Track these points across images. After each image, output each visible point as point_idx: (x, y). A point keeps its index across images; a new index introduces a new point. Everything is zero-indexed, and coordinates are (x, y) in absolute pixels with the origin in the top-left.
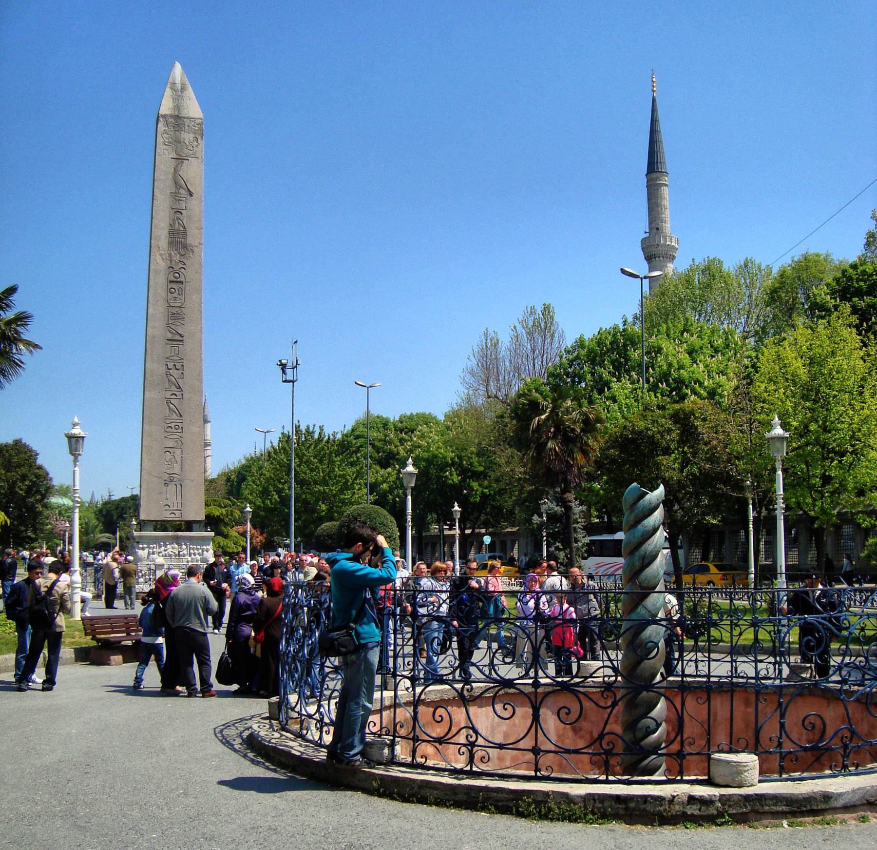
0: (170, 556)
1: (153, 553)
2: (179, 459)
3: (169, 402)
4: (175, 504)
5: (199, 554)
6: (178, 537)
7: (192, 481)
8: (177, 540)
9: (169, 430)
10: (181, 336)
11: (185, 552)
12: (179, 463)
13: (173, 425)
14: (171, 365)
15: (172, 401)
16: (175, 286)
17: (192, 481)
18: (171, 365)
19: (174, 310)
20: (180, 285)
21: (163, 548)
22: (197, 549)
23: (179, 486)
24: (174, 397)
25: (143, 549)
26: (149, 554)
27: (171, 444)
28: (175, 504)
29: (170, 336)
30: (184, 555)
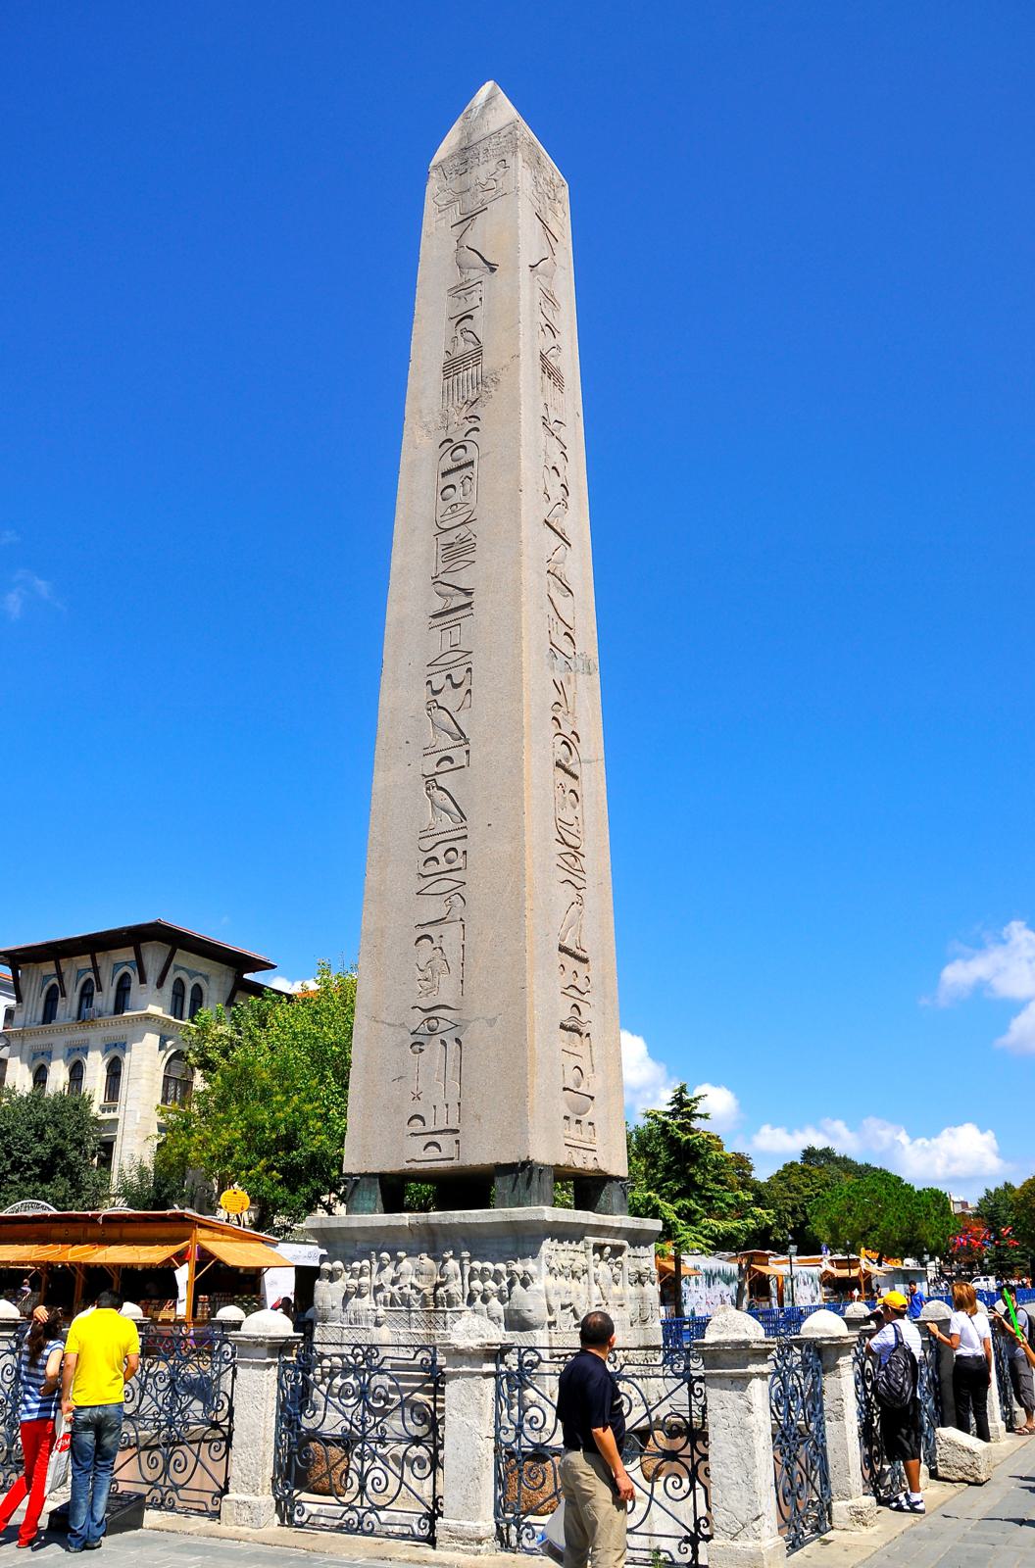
0: (406, 1301)
1: (359, 1294)
2: (453, 955)
3: (430, 781)
4: (442, 1111)
6: (430, 1230)
7: (492, 1022)
8: (433, 1242)
9: (433, 867)
10: (468, 593)
12: (455, 966)
13: (439, 852)
14: (439, 681)
15: (441, 780)
16: (452, 479)
17: (492, 1022)
18: (439, 681)
19: (450, 537)
20: (466, 471)
21: (390, 1272)
23: (452, 1045)
24: (446, 765)
26: (346, 1298)
27: (433, 909)
28: (442, 1111)
29: (439, 604)
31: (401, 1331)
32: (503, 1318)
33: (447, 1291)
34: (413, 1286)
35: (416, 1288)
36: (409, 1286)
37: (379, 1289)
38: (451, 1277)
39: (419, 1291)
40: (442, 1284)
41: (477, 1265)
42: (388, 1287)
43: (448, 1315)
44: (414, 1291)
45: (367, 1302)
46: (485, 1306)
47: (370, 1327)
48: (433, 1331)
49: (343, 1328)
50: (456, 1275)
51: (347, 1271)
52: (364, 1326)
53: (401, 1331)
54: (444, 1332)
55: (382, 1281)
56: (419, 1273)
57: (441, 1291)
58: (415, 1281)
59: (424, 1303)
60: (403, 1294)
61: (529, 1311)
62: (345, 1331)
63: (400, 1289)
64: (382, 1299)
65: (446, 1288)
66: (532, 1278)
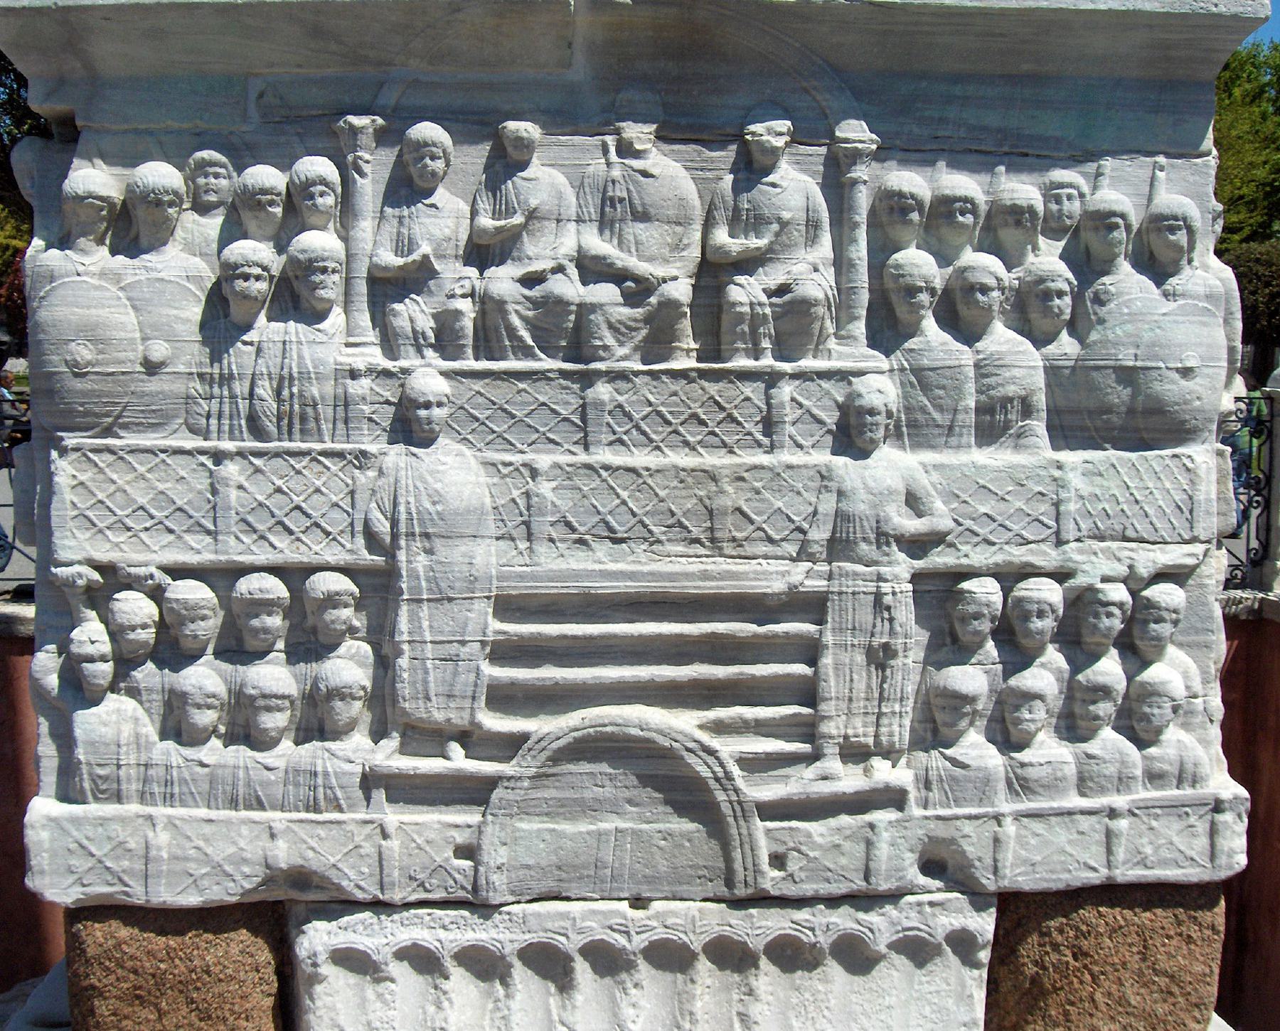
0: (568, 334)
1: (295, 296)
5: (1030, 310)
11: (810, 271)
21: (446, 218)
22: (1005, 228)
25: (133, 226)
26: (223, 318)
30: (794, 323)
31: (543, 461)
32: (1041, 400)
33: (783, 290)
34: (592, 269)
35: (619, 276)
36: (573, 271)
37: (388, 288)
38: (798, 234)
39: (637, 289)
40: (749, 264)
41: (910, 181)
42: (456, 275)
43: (786, 391)
44: (606, 293)
45: (337, 344)
46: (964, 356)
47: (372, 448)
48: (712, 459)
49: (219, 457)
50: (813, 226)
51: (202, 208)
52: (329, 445)
53: (543, 461)
54: (765, 459)
55: (425, 248)
56: (612, 211)
57: (746, 292)
58: (598, 244)
59: (658, 342)
60: (553, 305)
61: (1186, 372)
62: (231, 469)
63: (530, 280)
64: (426, 324)
65: (773, 276)
66: (1191, 247)
